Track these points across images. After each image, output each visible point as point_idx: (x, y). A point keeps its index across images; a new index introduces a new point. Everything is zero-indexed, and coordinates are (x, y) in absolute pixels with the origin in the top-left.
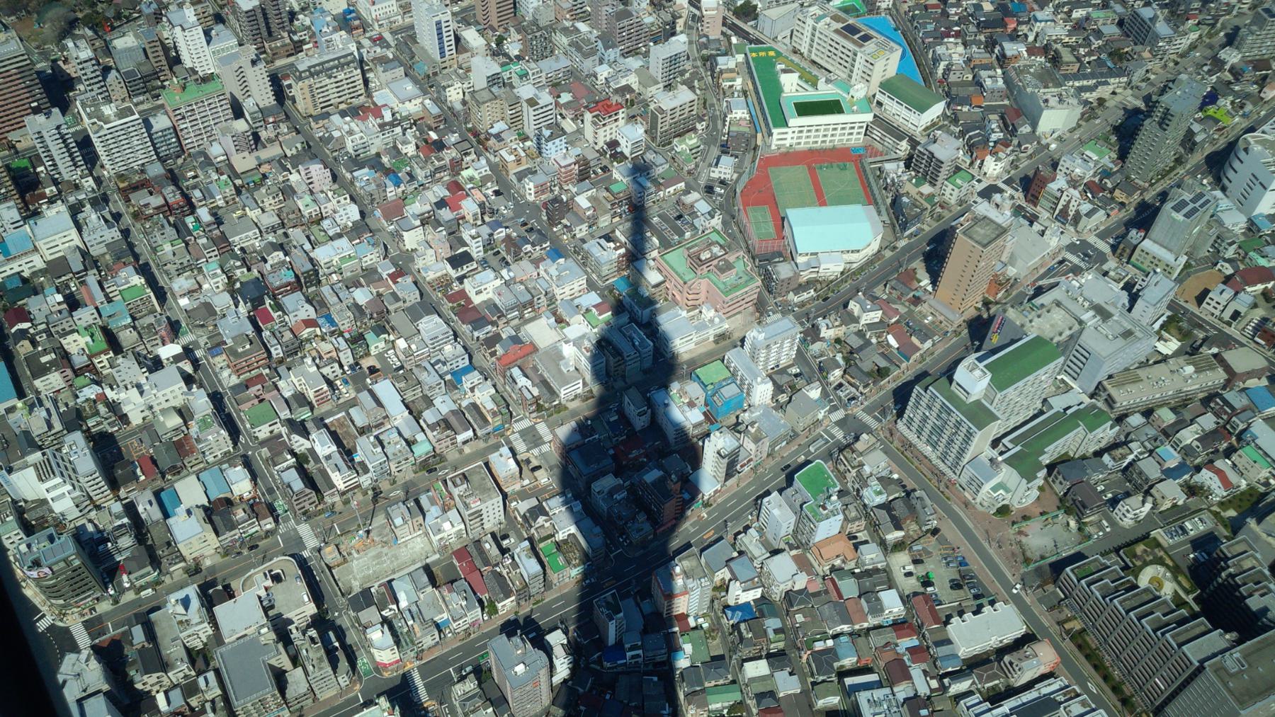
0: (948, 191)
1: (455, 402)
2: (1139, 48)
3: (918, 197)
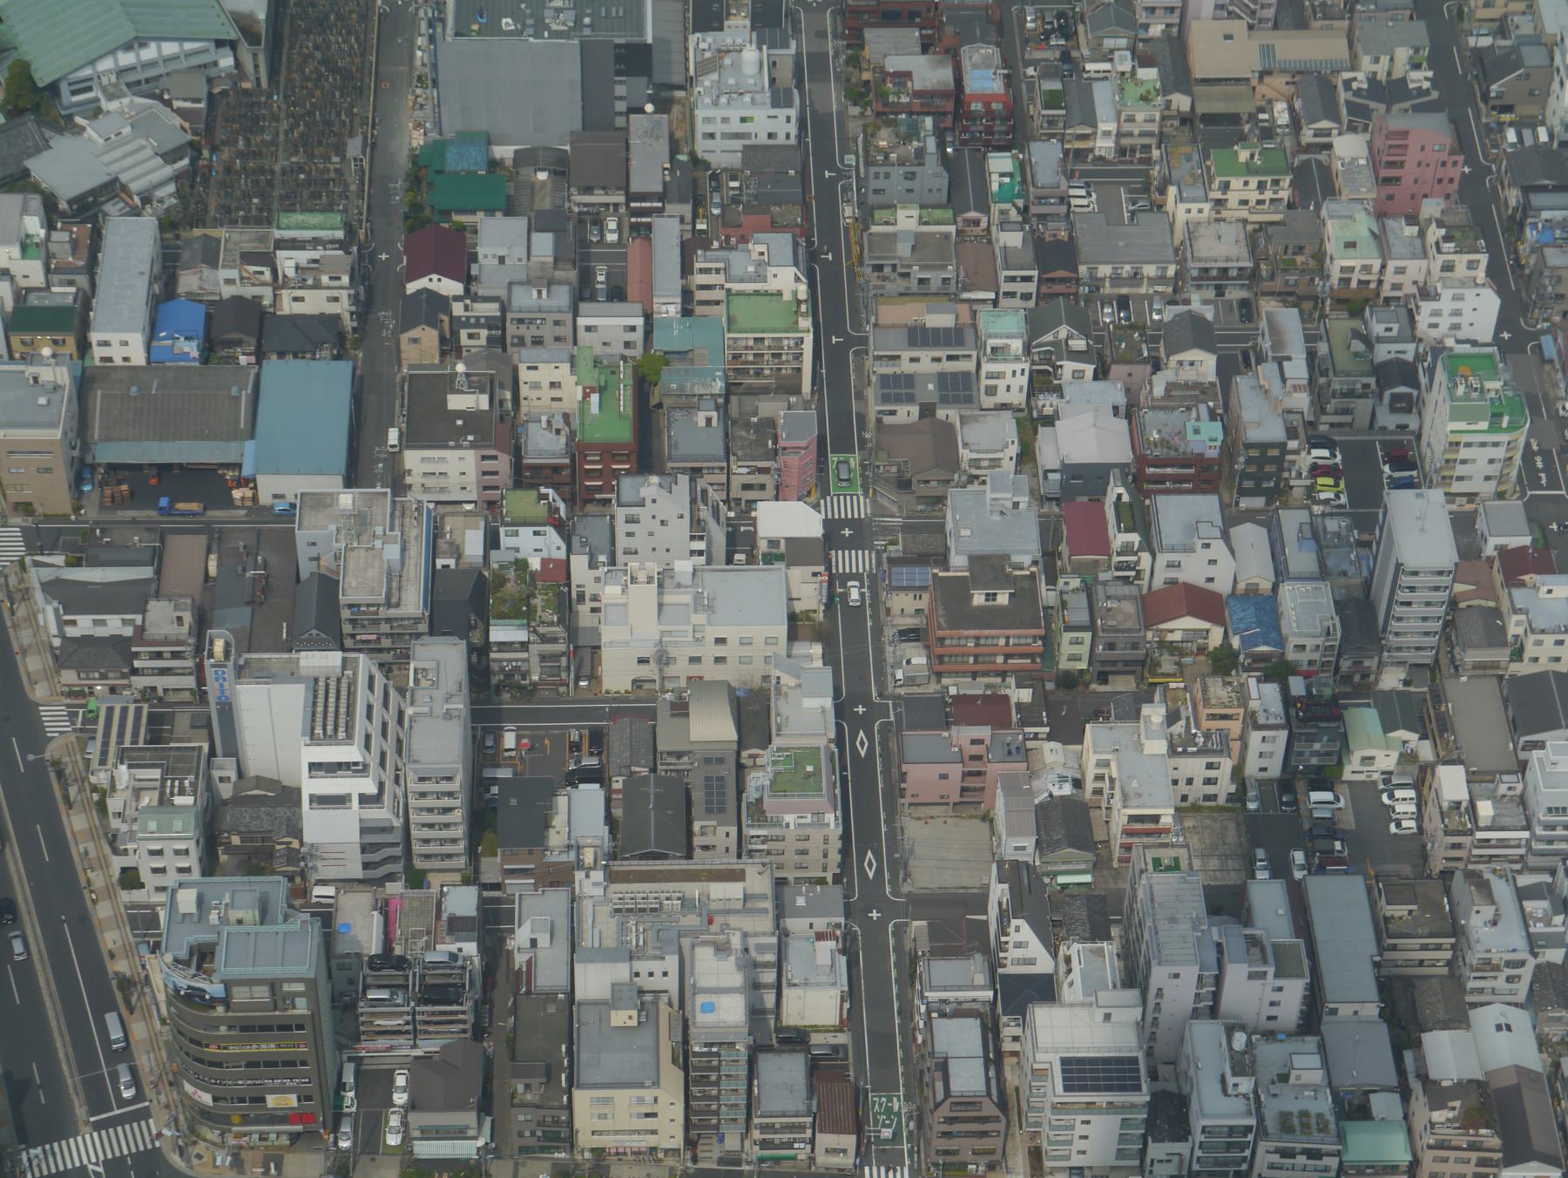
1: (1543, 1043)
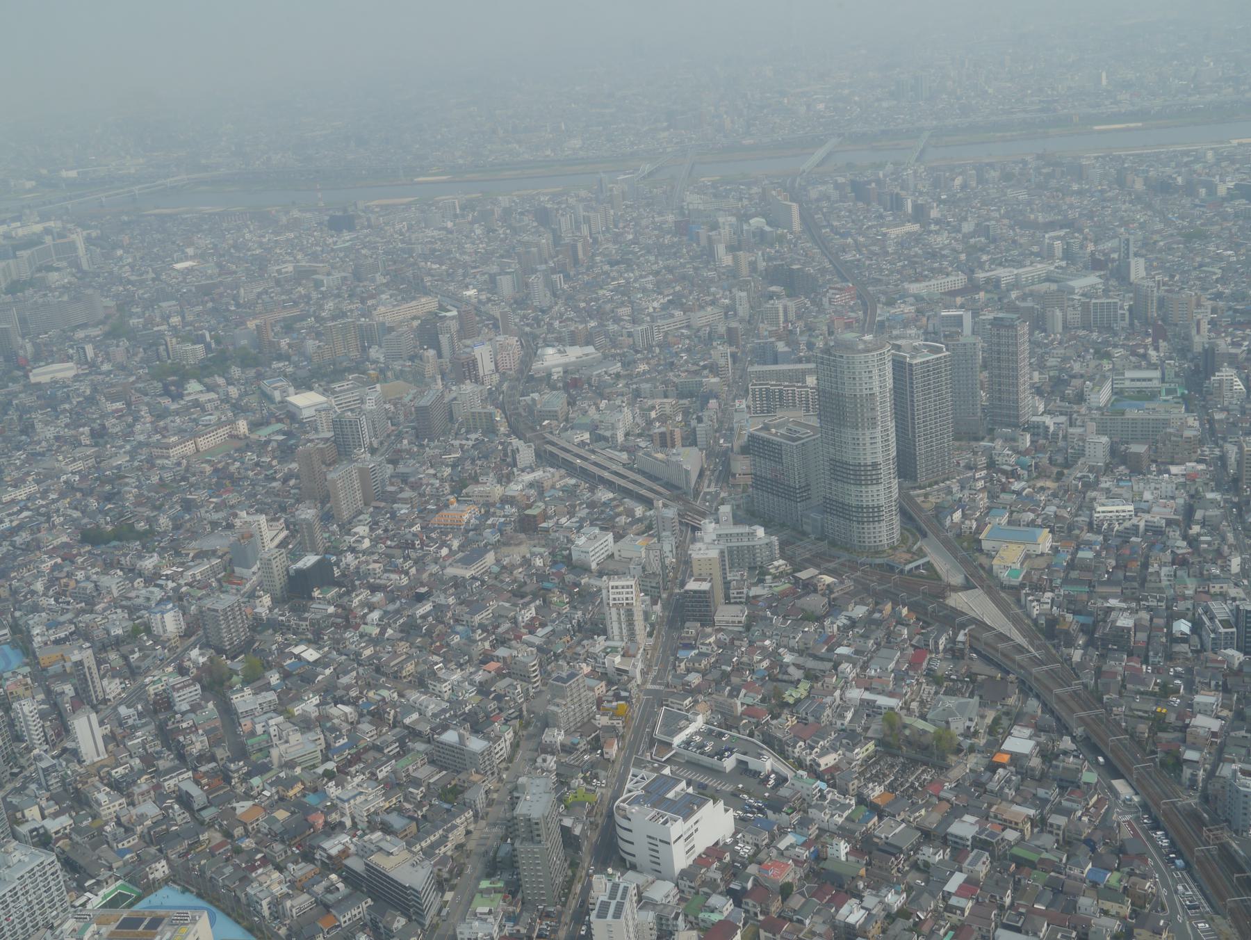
2: (463, 776)
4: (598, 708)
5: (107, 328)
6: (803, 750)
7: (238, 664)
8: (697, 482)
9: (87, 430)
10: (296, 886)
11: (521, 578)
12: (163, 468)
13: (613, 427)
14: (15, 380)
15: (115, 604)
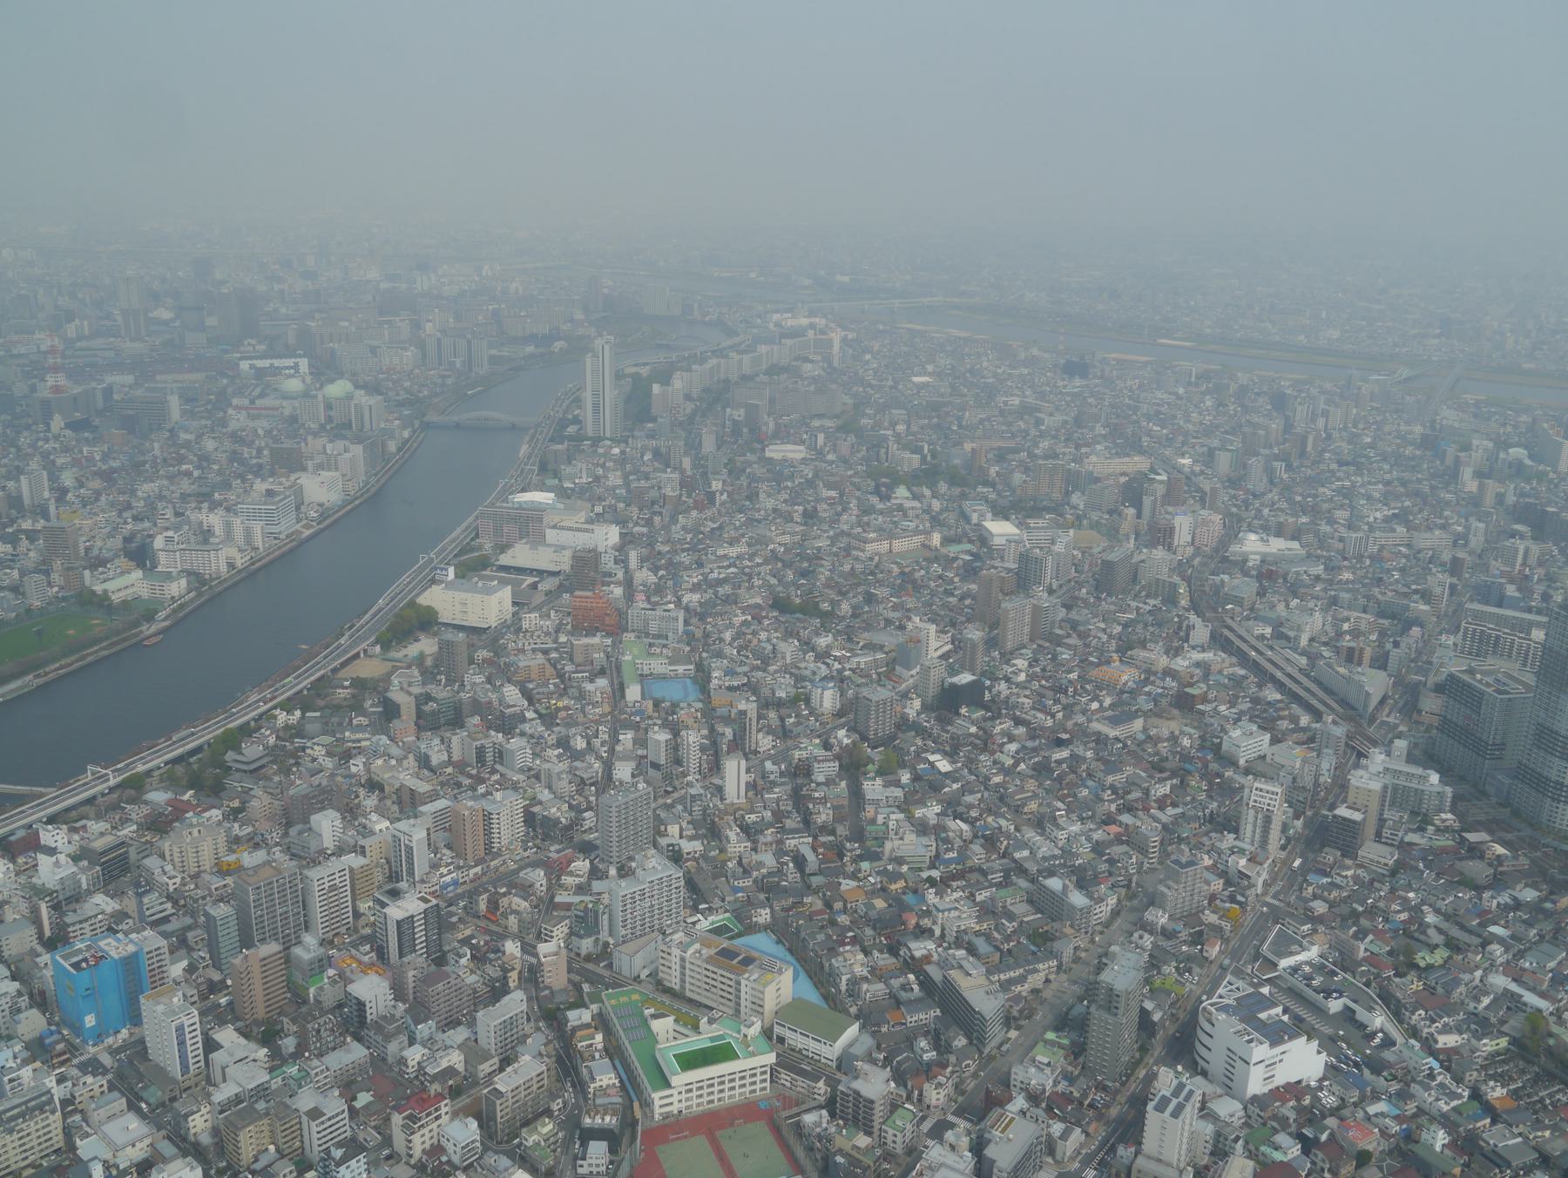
0: (890, 1138)
2: (1056, 925)
3: (854, 1153)
4: (1210, 904)
5: (840, 422)
6: (1423, 1019)
7: (877, 754)
8: (1376, 708)
9: (801, 508)
10: (876, 973)
11: (1164, 752)
12: (857, 559)
13: (1299, 629)
14: (753, 451)
15: (785, 669)
